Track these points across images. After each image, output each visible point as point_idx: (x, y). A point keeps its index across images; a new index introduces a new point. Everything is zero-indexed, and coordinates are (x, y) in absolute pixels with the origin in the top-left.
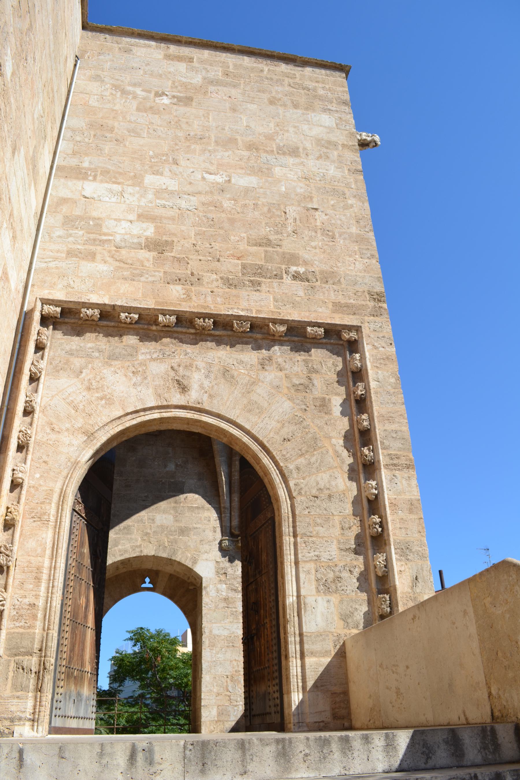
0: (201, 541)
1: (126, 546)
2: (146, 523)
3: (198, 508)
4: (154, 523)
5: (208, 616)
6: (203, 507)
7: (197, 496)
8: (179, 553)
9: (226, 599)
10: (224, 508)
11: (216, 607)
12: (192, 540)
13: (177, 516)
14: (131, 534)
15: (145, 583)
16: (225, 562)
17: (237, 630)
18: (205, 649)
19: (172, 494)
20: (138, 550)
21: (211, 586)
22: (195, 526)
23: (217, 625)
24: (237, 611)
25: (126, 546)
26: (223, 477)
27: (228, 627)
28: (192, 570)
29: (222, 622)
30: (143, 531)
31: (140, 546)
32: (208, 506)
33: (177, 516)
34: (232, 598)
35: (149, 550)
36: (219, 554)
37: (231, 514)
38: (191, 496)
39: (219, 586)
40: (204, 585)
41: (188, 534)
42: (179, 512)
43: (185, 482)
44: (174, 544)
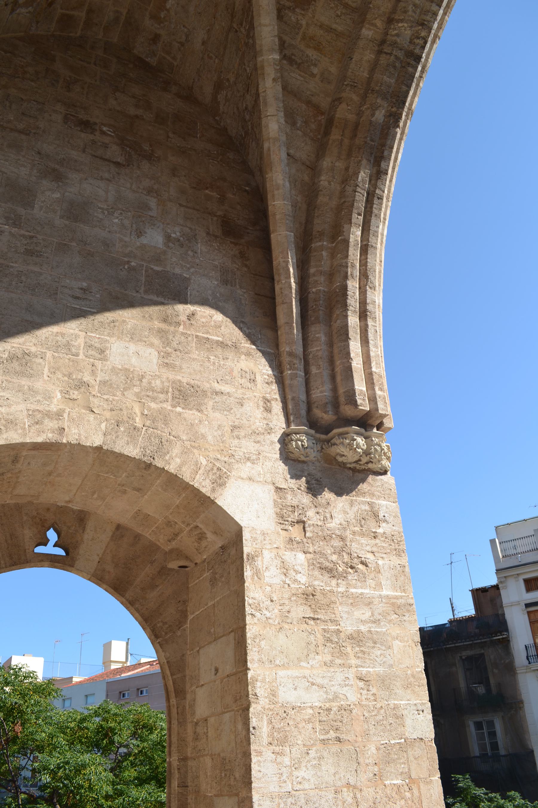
0: (234, 428)
1: (13, 409)
2: (81, 356)
3: (222, 345)
4: (104, 359)
5: (263, 643)
6: (235, 346)
7: (219, 317)
8: (176, 451)
9: (309, 596)
10: (291, 354)
11: (285, 616)
12: (211, 423)
13: (168, 354)
14: (31, 376)
15: (45, 542)
16: (297, 493)
17: (345, 690)
18: (260, 753)
19: (155, 298)
20: (50, 424)
21: (267, 555)
22: (218, 387)
23: (289, 672)
24: (338, 632)
25: (13, 409)
26: (292, 280)
27: (319, 681)
28: (213, 502)
29: (303, 664)
30: (69, 376)
31: (59, 415)
32: (246, 345)
33: (168, 354)
34: (323, 593)
35: (88, 431)
36: (282, 468)
37: (307, 372)
38: (208, 315)
39: (288, 556)
40: (247, 550)
41: (200, 404)
42: (174, 344)
43: (189, 279)
44: (160, 425)
